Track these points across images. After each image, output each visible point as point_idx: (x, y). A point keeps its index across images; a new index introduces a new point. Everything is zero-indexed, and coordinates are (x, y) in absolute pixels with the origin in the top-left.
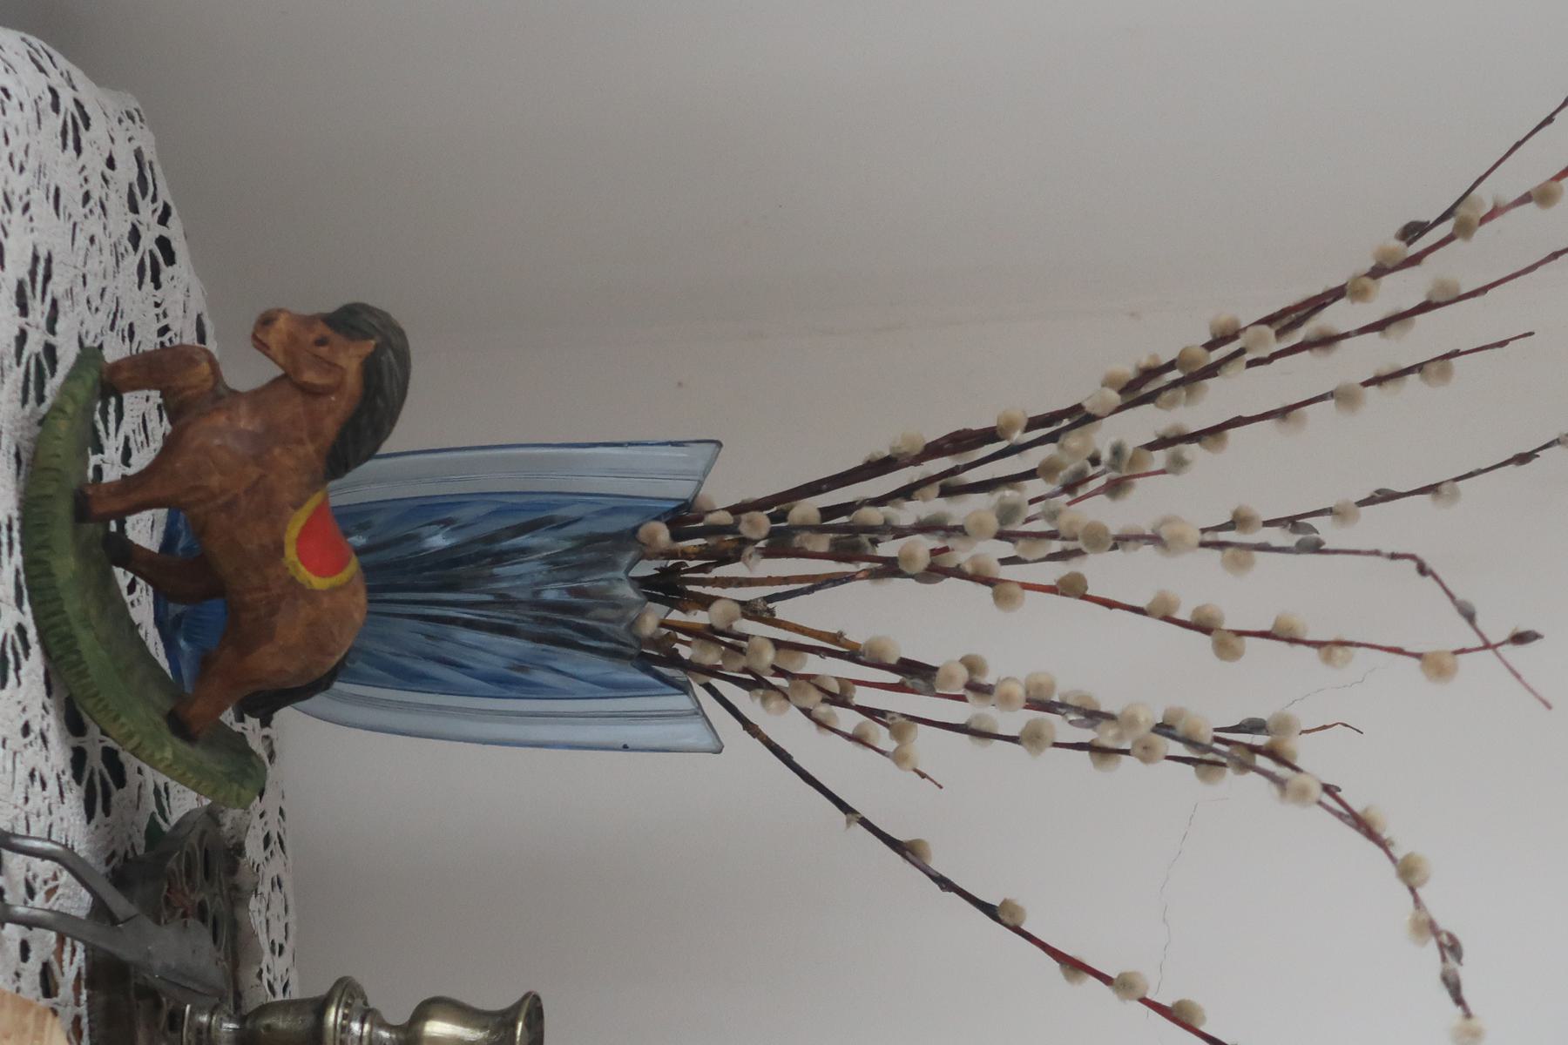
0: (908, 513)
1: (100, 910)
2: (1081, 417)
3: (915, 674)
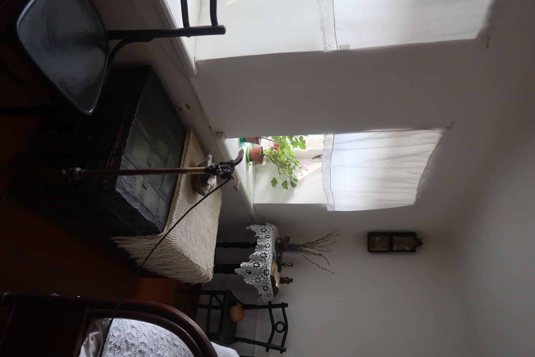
0: (307, 245)
1: (277, 258)
2: (314, 242)
3: (307, 252)
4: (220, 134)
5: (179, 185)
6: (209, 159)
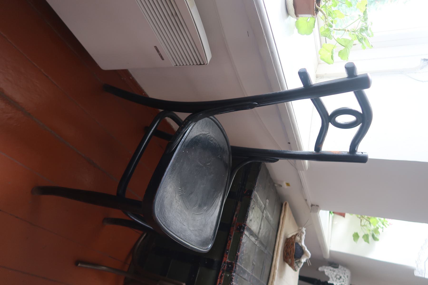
4: (315, 207)
5: (275, 266)
6: (303, 233)
